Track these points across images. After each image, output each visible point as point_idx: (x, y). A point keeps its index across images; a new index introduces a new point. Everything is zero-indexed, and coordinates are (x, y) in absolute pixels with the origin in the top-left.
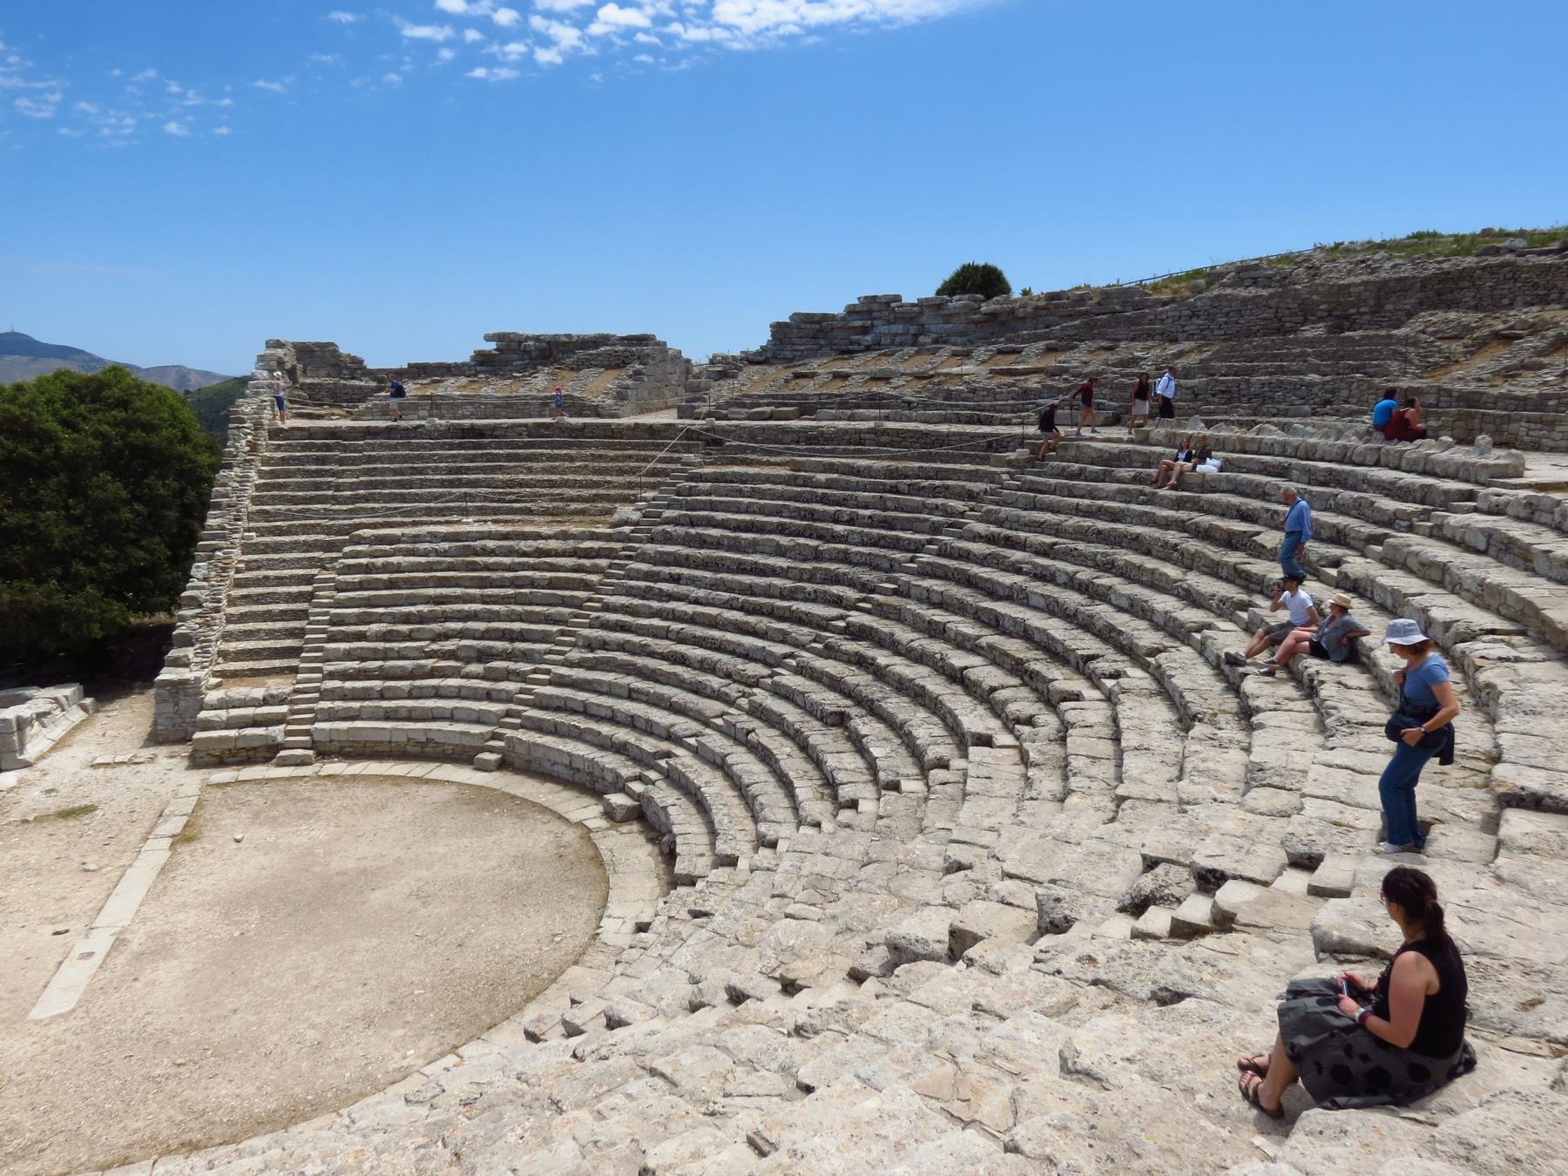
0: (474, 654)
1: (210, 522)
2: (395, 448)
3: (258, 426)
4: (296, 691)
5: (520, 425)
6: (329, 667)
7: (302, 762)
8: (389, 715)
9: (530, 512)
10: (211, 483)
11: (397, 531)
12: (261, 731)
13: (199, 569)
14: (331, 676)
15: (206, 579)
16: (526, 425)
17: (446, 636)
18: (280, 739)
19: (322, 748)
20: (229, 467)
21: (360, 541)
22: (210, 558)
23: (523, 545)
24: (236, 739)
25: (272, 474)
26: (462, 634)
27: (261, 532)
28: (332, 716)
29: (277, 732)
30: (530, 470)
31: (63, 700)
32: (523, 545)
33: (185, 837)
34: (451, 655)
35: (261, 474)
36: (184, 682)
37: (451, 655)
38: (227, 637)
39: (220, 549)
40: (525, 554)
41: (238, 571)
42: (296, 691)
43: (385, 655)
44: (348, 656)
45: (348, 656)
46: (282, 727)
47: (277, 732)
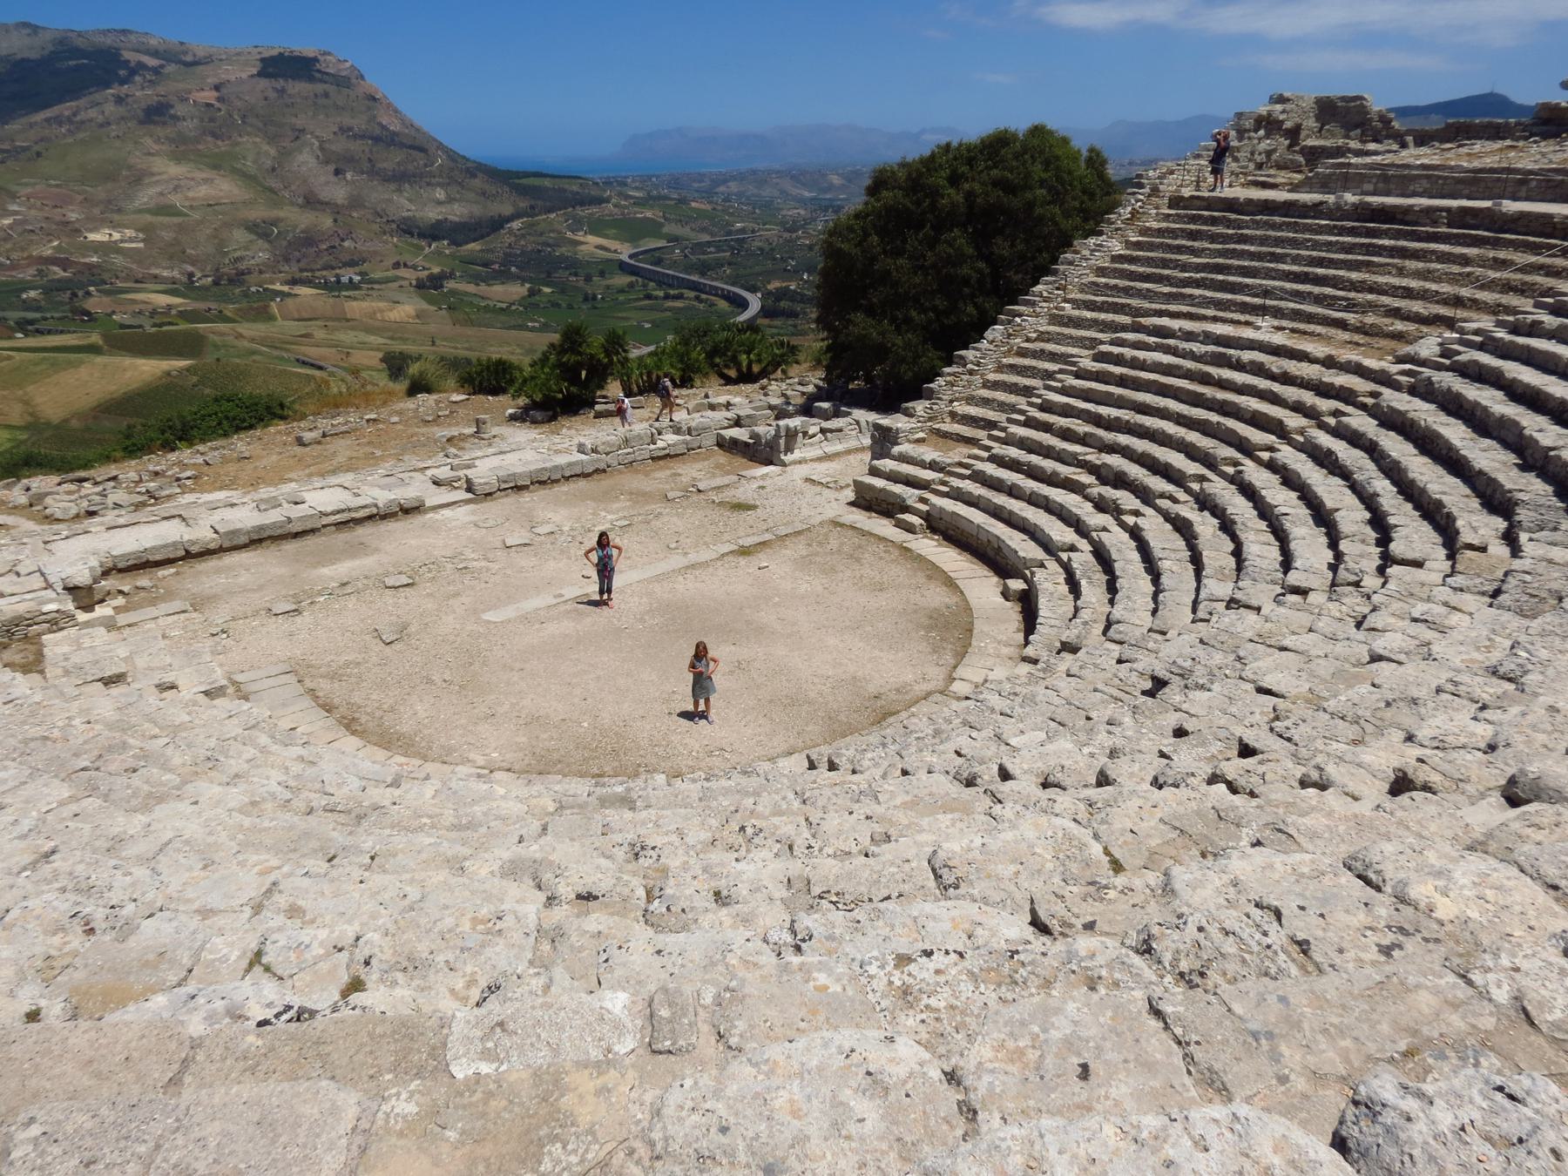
0: (1111, 477)
1: (1039, 288)
2: (1278, 227)
3: (1155, 191)
4: (961, 464)
5: (1441, 209)
6: (998, 449)
7: (910, 529)
8: (997, 513)
9: (1342, 325)
10: (1066, 244)
11: (1175, 324)
12: (898, 489)
13: (996, 332)
14: (994, 459)
15: (991, 342)
16: (1448, 210)
17: (1112, 449)
18: (909, 502)
19: (934, 524)
20: (1100, 233)
21: (1137, 328)
22: (1009, 322)
23: (1275, 364)
24: (883, 490)
25: (1138, 246)
26: (1126, 452)
27: (1076, 304)
28: (957, 495)
29: (910, 495)
30: (1401, 272)
31: (863, 424)
32: (1275, 364)
33: (744, 552)
34: (1092, 469)
35: (1129, 245)
36: (889, 429)
37: (1092, 469)
38: (970, 400)
39: (1020, 315)
40: (1272, 377)
41: (1028, 340)
42: (961, 464)
43: (1048, 452)
44: (1022, 444)
45: (1022, 444)
46: (917, 492)
47: (910, 495)
